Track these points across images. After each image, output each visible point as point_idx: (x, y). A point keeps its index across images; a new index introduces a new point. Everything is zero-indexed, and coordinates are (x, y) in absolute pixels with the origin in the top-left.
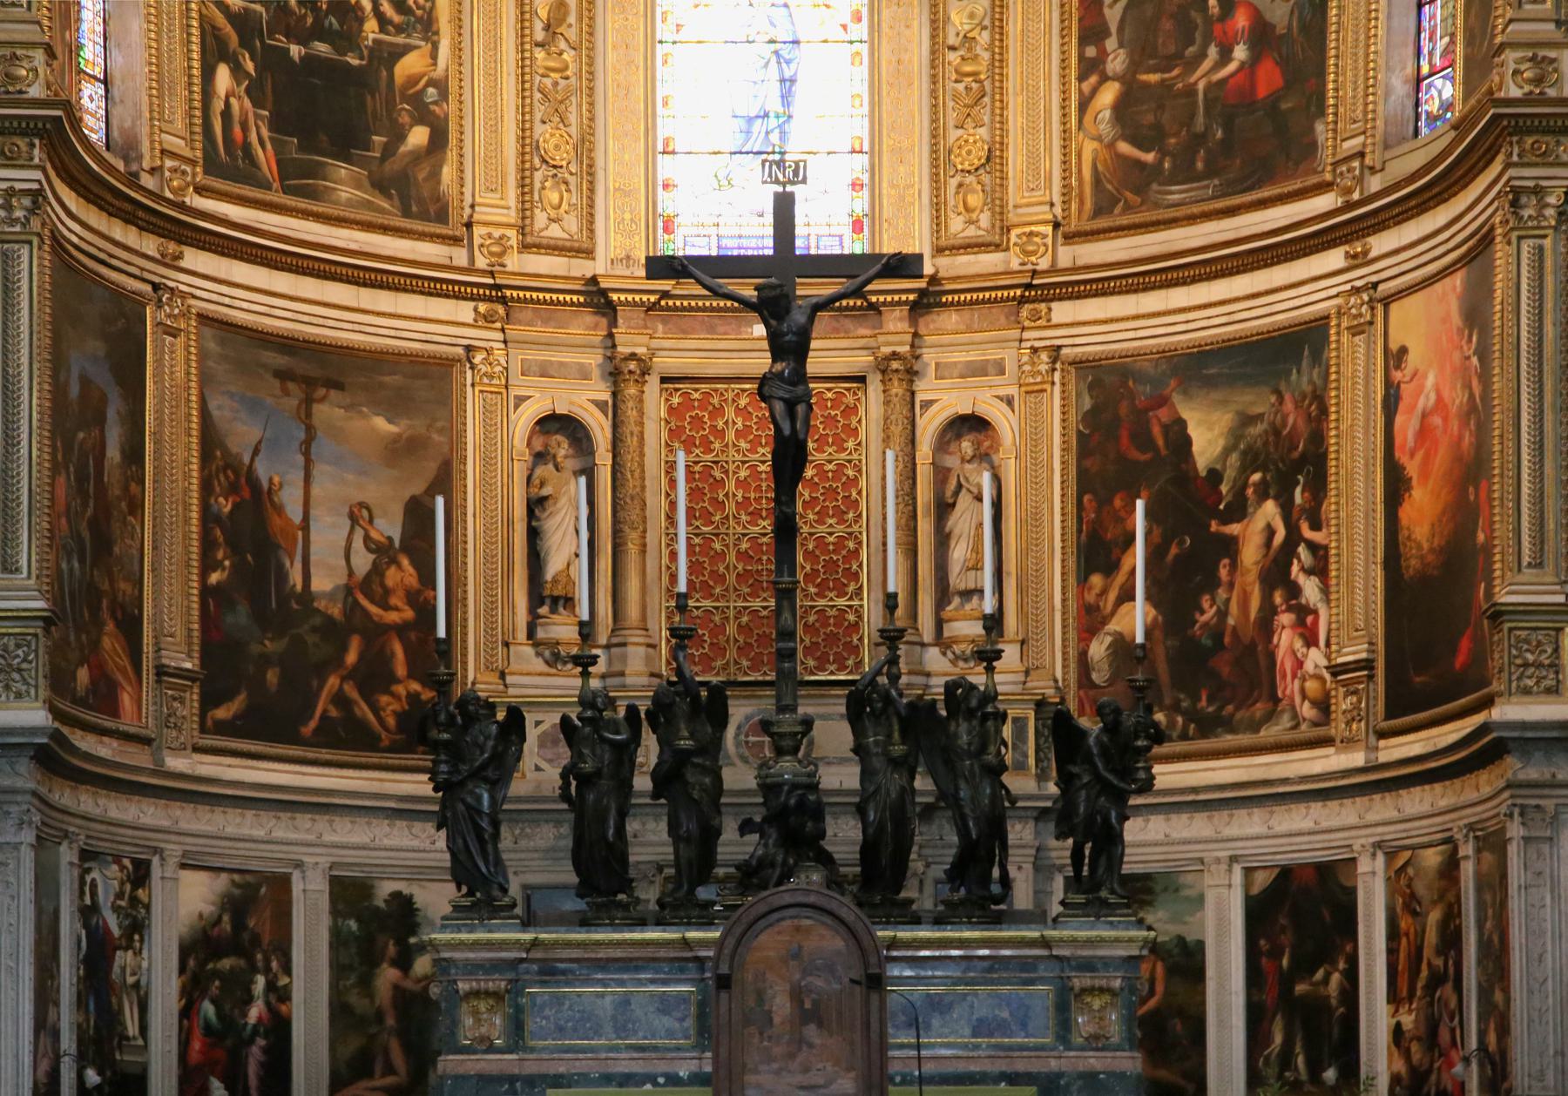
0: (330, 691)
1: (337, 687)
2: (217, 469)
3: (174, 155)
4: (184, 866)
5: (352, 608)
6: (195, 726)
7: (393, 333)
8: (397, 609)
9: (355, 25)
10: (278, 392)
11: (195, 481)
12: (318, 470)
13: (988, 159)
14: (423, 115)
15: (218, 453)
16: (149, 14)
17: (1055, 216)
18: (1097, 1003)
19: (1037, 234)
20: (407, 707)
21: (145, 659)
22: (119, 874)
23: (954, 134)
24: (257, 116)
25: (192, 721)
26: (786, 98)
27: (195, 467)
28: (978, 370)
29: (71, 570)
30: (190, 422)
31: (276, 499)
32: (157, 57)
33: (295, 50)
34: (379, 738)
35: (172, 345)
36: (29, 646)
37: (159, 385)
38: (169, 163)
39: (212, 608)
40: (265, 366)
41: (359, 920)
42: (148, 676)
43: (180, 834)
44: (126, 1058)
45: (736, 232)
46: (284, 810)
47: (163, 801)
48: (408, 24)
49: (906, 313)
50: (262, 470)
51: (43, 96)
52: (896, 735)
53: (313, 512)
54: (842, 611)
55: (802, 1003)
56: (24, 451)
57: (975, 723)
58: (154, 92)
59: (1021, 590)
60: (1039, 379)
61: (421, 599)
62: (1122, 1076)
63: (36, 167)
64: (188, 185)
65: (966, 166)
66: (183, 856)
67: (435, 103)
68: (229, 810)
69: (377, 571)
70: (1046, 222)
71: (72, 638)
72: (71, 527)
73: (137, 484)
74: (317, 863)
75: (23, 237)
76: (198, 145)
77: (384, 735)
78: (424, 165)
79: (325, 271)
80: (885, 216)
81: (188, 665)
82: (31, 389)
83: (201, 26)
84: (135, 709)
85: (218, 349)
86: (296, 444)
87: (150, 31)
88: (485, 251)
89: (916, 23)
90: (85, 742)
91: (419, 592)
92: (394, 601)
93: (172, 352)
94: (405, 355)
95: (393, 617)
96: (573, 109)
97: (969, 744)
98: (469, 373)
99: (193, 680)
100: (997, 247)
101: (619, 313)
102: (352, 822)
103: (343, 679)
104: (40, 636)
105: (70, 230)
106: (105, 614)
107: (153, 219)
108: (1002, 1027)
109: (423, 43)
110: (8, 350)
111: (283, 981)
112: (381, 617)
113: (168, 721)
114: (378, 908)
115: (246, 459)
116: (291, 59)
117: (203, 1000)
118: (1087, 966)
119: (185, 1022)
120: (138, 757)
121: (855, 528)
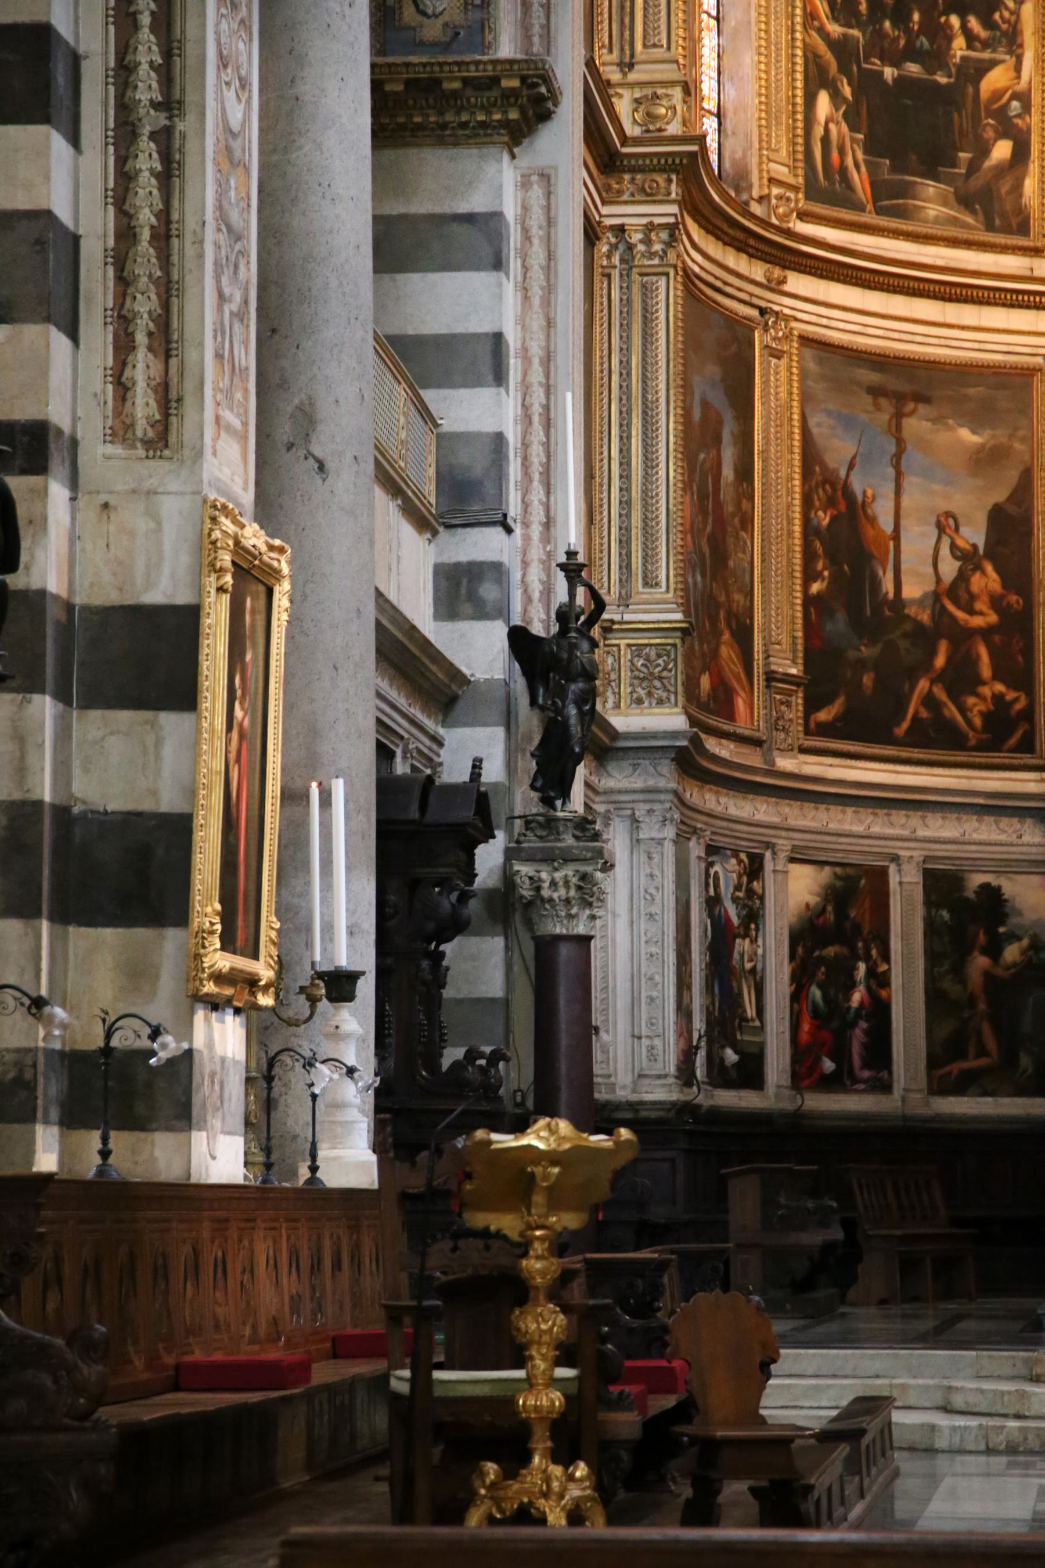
0: (920, 694)
1: (926, 690)
2: (817, 487)
3: (780, 183)
5: (940, 614)
6: (801, 728)
7: (976, 346)
8: (981, 613)
10: (871, 408)
11: (797, 496)
12: (910, 482)
14: (1008, 129)
15: (817, 469)
16: (760, 46)
20: (992, 707)
21: (756, 666)
22: (737, 867)
24: (853, 140)
25: (798, 724)
27: (797, 483)
29: (695, 584)
30: (792, 439)
31: (869, 511)
32: (766, 88)
33: (889, 73)
34: (966, 738)
35: (777, 367)
36: (669, 656)
37: (766, 405)
38: (776, 191)
39: (813, 616)
41: (951, 911)
42: (759, 682)
46: (882, 808)
47: (774, 799)
48: (994, 39)
50: (857, 485)
51: (680, 133)
53: (904, 523)
56: (662, 473)
58: (763, 122)
61: (1004, 603)
64: (792, 211)
66: (792, 851)
67: (1019, 116)
68: (832, 807)
69: (962, 578)
71: (697, 647)
72: (694, 542)
74: (912, 857)
75: (660, 270)
76: (800, 172)
77: (971, 734)
78: (1008, 178)
79: (914, 288)
81: (794, 671)
82: (668, 413)
83: (805, 56)
84: (748, 711)
86: (887, 458)
87: (760, 62)
90: (712, 744)
91: (1002, 597)
92: (979, 606)
93: (777, 373)
94: (988, 367)
95: (977, 621)
99: (798, 685)
102: (943, 818)
103: (933, 682)
104: (679, 646)
105: (693, 261)
106: (722, 625)
107: (767, 249)
109: (1007, 57)
110: (647, 377)
111: (884, 967)
112: (967, 622)
113: (777, 724)
114: (967, 899)
115: (843, 474)
116: (885, 82)
117: (810, 985)
119: (796, 1006)
120: (752, 758)
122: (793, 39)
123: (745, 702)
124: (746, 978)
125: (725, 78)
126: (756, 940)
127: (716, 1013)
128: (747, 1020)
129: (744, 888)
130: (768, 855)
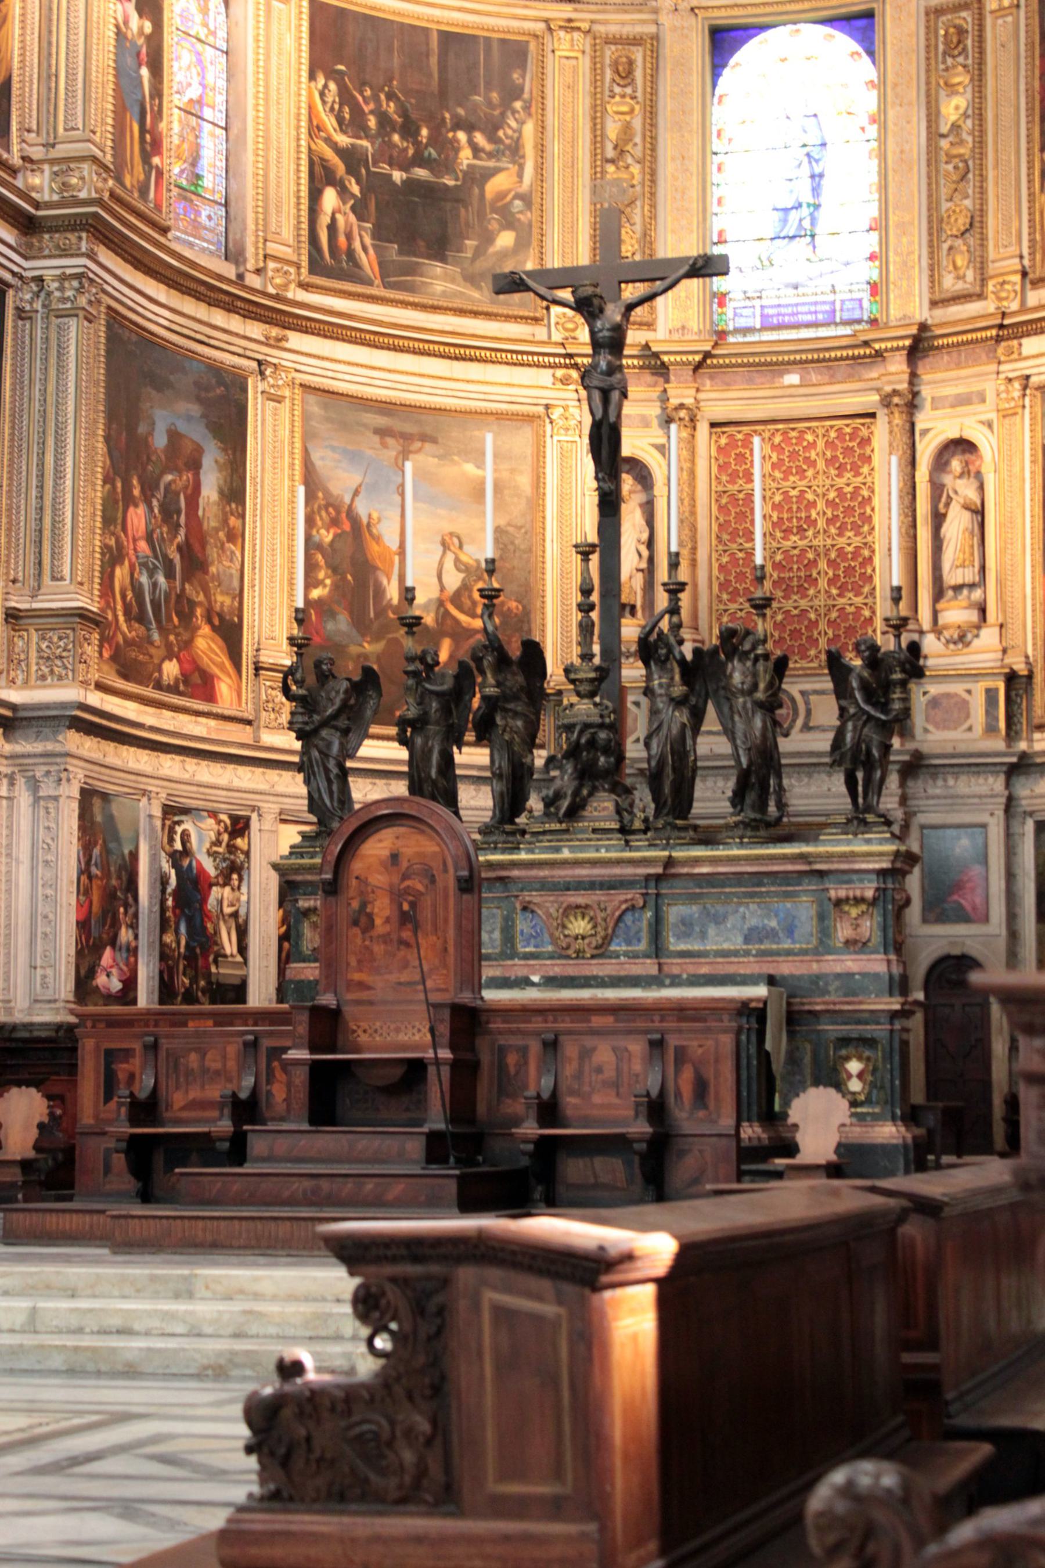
2: (320, 508)
3: (275, 258)
4: (284, 821)
5: (444, 616)
7: (482, 396)
9: (452, 154)
10: (378, 446)
13: (971, 225)
15: (320, 495)
17: (1023, 267)
18: (854, 912)
19: (1008, 283)
23: (945, 206)
24: (360, 228)
26: (816, 190)
28: (963, 401)
29: (155, 585)
31: (374, 531)
33: (398, 176)
36: (67, 637)
38: (272, 265)
39: (313, 617)
40: (365, 426)
43: (277, 795)
44: (222, 971)
45: (776, 302)
48: (498, 151)
49: (905, 358)
50: (362, 509)
52: (677, 677)
54: (859, 609)
55: (401, 905)
57: (749, 664)
59: (999, 582)
60: (1013, 404)
61: (505, 608)
62: (876, 976)
63: (83, 255)
65: (955, 232)
67: (521, 212)
70: (1015, 272)
73: (237, 518)
75: (72, 312)
80: (892, 278)
84: (235, 695)
85: (322, 412)
86: (393, 487)
88: (560, 327)
89: (915, 119)
96: (638, 211)
97: (743, 683)
98: (548, 427)
100: (980, 296)
101: (672, 373)
108: (771, 935)
109: (510, 166)
115: (347, 500)
116: (394, 184)
118: (845, 876)
121: (869, 539)
122: (299, 146)
123: (230, 687)
124: (225, 921)
125: (231, 174)
126: (239, 888)
127: (182, 950)
128: (225, 956)
129: (224, 844)
130: (254, 816)
